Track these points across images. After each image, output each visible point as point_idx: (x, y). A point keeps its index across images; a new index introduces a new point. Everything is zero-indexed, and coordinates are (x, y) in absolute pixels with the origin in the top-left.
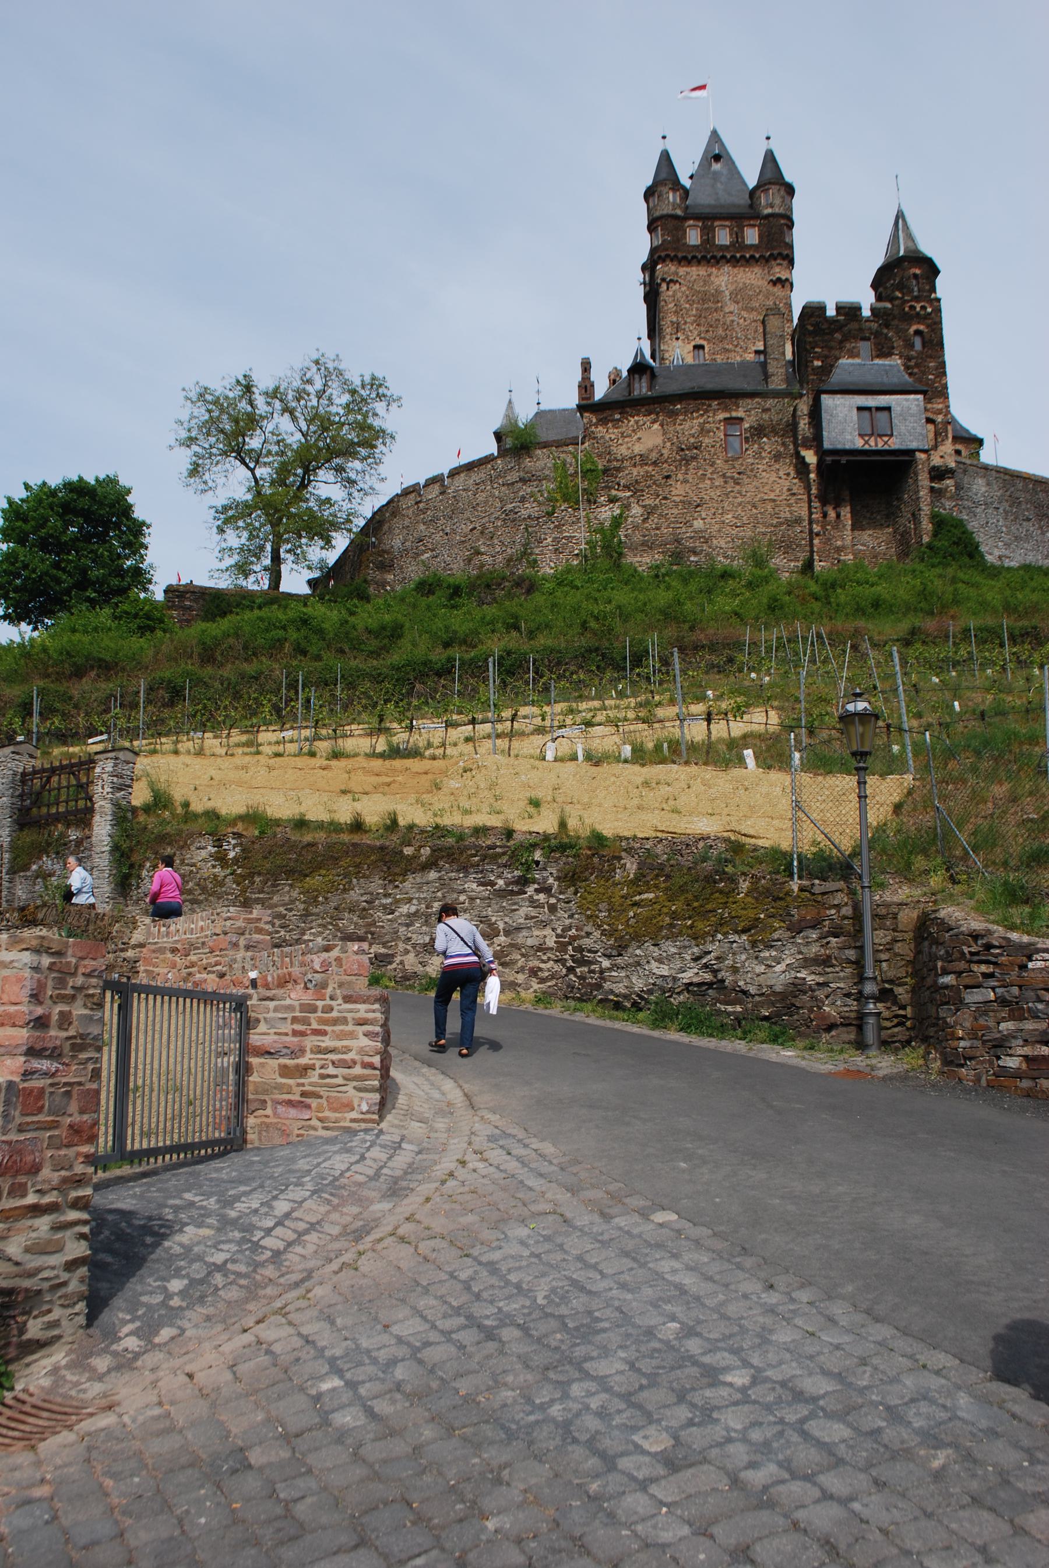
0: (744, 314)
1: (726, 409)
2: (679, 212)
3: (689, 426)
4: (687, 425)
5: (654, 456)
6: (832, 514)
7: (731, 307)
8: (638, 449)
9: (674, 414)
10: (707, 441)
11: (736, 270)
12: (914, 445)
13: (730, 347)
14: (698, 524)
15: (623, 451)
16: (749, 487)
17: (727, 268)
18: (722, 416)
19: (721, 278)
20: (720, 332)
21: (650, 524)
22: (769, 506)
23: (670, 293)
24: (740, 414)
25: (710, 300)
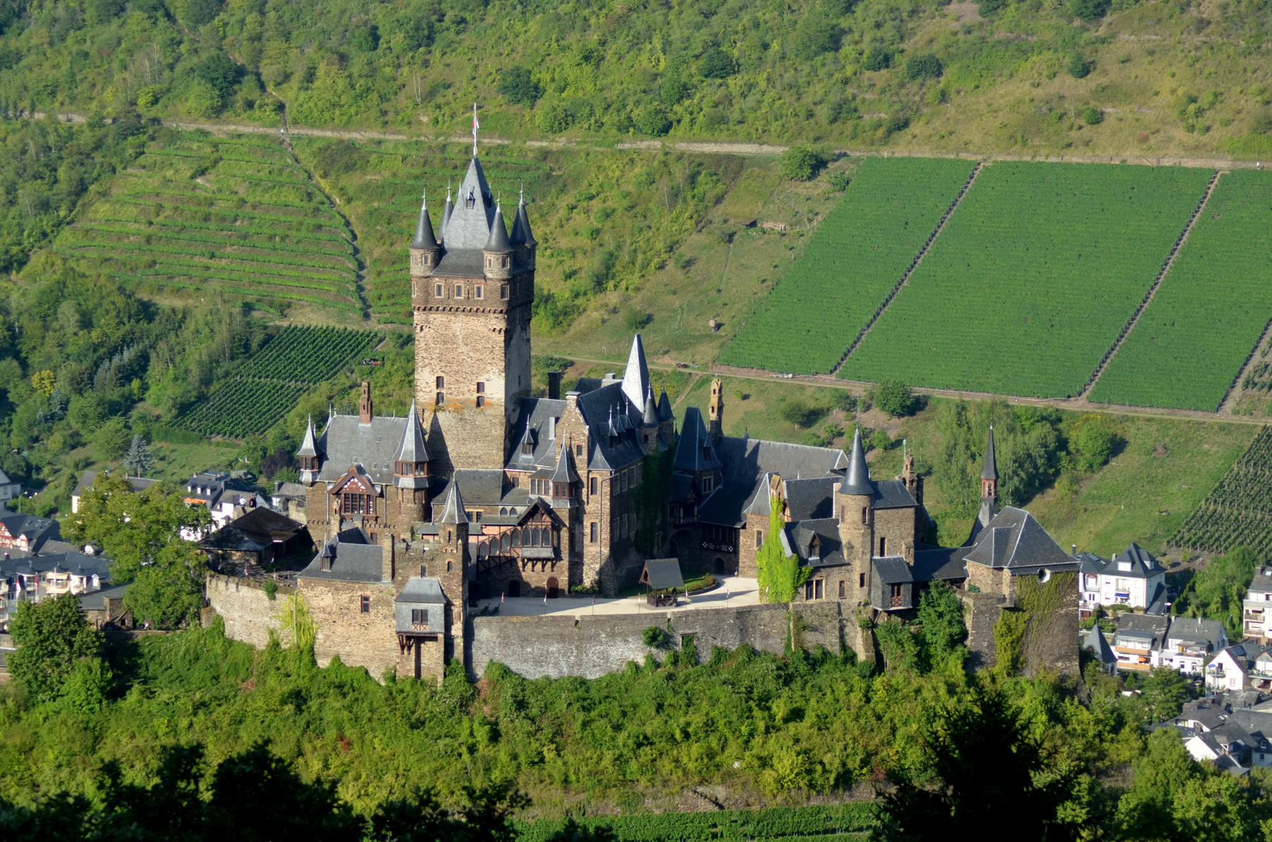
0: (471, 354)
1: (360, 589)
2: (428, 273)
3: (344, 598)
4: (344, 596)
5: (328, 610)
6: (406, 651)
7: (463, 349)
8: (322, 604)
9: (337, 589)
10: (352, 606)
11: (467, 319)
12: (437, 630)
13: (461, 379)
14: (347, 649)
15: (314, 603)
16: (372, 630)
17: (461, 316)
18: (360, 593)
19: (458, 324)
20: (455, 367)
21: (328, 643)
22: (381, 642)
23: (422, 334)
24: (368, 593)
25: (447, 341)
